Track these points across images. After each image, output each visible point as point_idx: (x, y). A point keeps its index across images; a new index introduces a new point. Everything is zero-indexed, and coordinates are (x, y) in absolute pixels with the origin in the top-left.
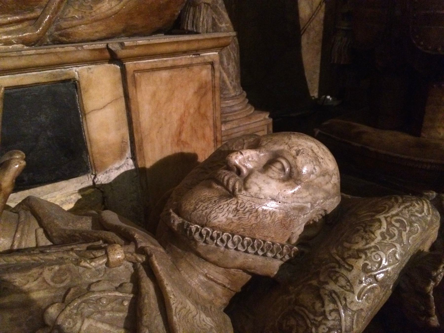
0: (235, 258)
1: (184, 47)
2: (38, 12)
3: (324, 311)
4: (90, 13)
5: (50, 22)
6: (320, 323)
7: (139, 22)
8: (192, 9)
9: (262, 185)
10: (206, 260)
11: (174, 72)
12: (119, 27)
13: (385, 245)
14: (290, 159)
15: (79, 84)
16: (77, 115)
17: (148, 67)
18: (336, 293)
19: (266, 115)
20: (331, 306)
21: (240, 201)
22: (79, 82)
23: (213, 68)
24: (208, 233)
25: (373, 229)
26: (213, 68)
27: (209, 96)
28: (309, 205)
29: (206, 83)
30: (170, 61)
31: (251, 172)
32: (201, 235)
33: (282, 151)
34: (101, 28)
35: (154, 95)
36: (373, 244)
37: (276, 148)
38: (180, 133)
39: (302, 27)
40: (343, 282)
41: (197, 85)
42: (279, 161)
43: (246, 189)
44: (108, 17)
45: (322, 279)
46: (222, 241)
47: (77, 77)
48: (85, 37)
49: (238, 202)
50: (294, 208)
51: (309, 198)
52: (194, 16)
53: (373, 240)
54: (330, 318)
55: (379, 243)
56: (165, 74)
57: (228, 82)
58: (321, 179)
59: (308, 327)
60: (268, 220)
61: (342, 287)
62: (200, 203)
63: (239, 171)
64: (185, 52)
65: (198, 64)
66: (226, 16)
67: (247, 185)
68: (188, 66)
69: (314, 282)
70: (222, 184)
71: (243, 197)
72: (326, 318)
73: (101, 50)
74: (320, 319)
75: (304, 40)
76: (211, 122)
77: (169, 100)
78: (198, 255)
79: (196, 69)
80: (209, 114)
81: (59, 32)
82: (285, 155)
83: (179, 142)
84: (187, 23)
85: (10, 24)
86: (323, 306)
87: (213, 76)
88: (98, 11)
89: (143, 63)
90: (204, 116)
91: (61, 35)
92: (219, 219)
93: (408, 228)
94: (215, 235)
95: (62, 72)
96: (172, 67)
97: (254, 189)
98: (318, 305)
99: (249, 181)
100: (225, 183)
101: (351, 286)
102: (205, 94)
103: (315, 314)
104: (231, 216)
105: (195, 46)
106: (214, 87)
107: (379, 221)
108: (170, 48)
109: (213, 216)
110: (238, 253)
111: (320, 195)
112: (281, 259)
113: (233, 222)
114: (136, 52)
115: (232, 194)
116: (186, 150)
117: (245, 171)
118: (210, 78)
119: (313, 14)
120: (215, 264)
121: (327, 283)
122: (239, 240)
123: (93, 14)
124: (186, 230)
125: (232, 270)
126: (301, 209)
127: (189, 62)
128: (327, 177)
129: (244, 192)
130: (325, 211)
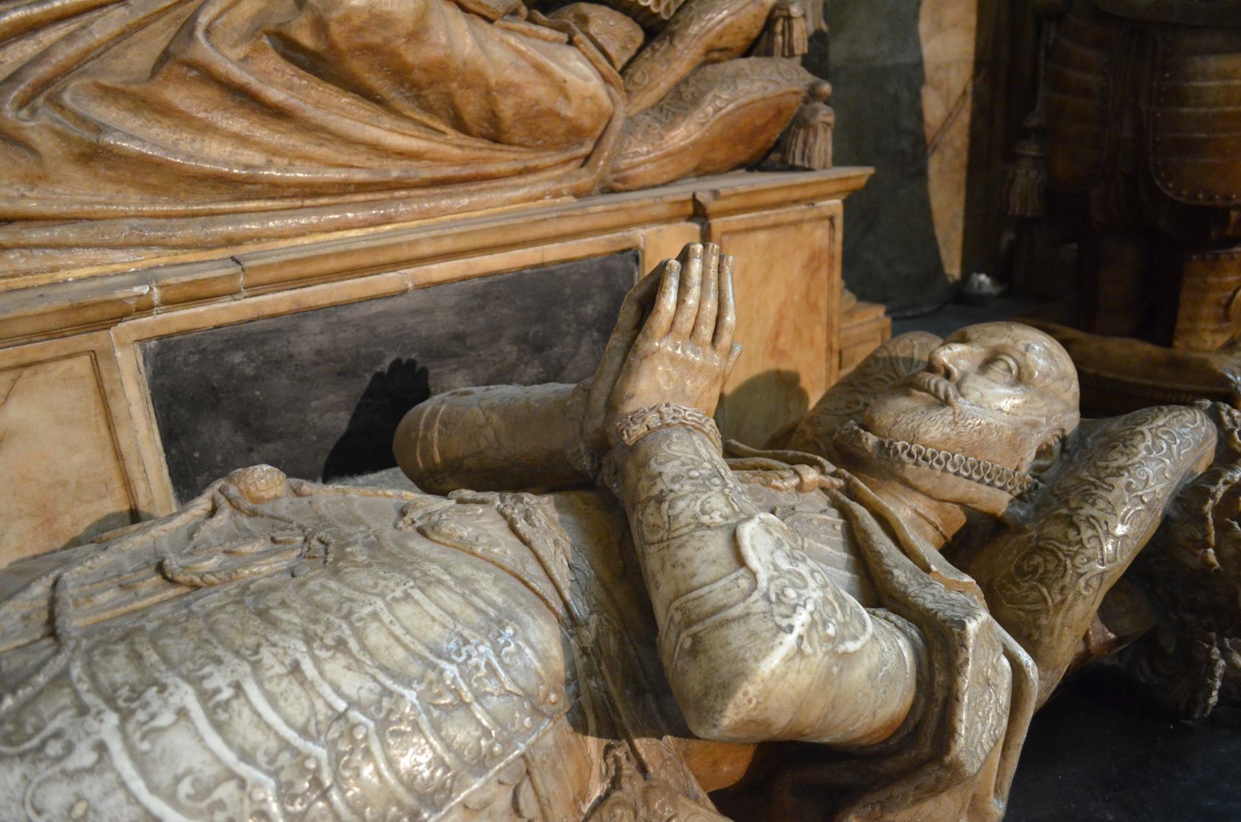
0: (955, 486)
1: (797, 194)
3: (1081, 540)
4: (660, 145)
6: (1077, 553)
8: (802, 132)
9: (985, 391)
10: (915, 489)
11: (776, 234)
12: (691, 163)
13: (1152, 460)
14: (1018, 356)
15: (643, 256)
17: (742, 226)
18: (1093, 517)
19: (879, 311)
20: (1090, 532)
21: (957, 411)
22: (643, 251)
23: (832, 226)
24: (919, 452)
25: (1135, 442)
26: (832, 226)
27: (824, 273)
28: (1044, 420)
30: (772, 216)
31: (964, 375)
32: (910, 455)
33: (1004, 346)
34: (671, 167)
36: (1136, 459)
37: (995, 342)
38: (777, 336)
39: (929, 139)
40: (1101, 504)
42: (1001, 360)
43: (963, 396)
44: (682, 150)
45: (1073, 505)
46: (939, 462)
47: (642, 246)
48: (649, 181)
49: (954, 413)
50: (1026, 424)
51: (1045, 410)
52: (805, 143)
53: (1136, 455)
54: (1088, 546)
55: (1145, 458)
56: (762, 237)
58: (1058, 384)
59: (1060, 560)
60: (994, 437)
61: (1102, 510)
62: (902, 415)
63: (948, 374)
64: (796, 202)
65: (811, 220)
67: (964, 391)
68: (797, 224)
69: (1064, 511)
70: (927, 390)
71: (962, 404)
72: (1083, 546)
73: (683, 203)
74: (1076, 548)
75: (934, 165)
76: (824, 318)
78: (905, 483)
80: (822, 304)
81: (615, 176)
82: (1010, 351)
83: (776, 352)
84: (794, 153)
86: (1079, 533)
87: (832, 239)
88: (671, 142)
89: (736, 220)
90: (814, 308)
91: (616, 180)
92: (932, 435)
93: (1178, 441)
94: (929, 455)
95: (624, 237)
96: (775, 226)
97: (974, 396)
98: (1072, 534)
99: (965, 385)
100: (933, 388)
101: (1113, 508)
102: (818, 268)
103: (1069, 544)
104: (947, 430)
105: (812, 191)
106: (832, 257)
107: (1142, 433)
108: (777, 197)
109: (922, 430)
110: (959, 479)
111: (1058, 407)
112: (1010, 492)
113: (949, 439)
115: (945, 402)
116: (785, 366)
117: (956, 373)
118: (826, 241)
119: (950, 114)
120: (928, 494)
121: (1081, 508)
122: (961, 461)
123: (665, 146)
124: (889, 449)
125: (948, 505)
126: (1034, 425)
127: (799, 217)
128: (1066, 381)
129: (961, 399)
130: (1063, 430)
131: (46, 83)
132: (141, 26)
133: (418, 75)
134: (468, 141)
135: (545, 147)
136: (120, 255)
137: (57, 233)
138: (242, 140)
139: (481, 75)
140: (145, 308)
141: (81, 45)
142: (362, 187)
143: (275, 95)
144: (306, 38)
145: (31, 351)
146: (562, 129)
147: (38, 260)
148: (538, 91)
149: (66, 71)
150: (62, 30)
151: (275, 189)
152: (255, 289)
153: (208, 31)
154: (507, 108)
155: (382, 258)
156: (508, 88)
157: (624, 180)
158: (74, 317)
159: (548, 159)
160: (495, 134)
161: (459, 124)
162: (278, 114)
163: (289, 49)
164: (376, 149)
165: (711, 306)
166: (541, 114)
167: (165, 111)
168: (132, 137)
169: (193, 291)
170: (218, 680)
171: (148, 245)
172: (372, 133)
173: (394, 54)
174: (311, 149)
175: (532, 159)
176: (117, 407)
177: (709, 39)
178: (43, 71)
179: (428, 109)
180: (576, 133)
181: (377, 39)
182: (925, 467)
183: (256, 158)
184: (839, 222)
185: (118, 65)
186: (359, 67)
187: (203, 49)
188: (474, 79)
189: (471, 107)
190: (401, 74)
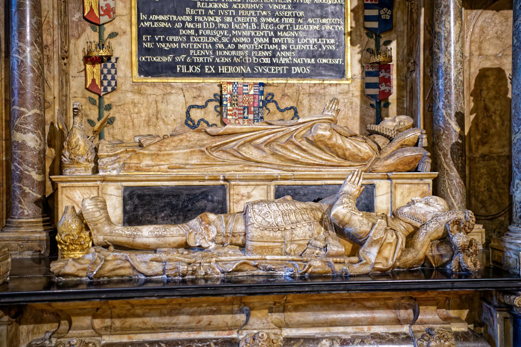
1: (416, 176)
2: (367, 162)
5: (370, 166)
7: (401, 167)
10: (400, 219)
12: (393, 169)
16: (373, 196)
29: (426, 192)
30: (410, 181)
35: (402, 193)
41: (421, 192)
44: (389, 165)
56: (408, 186)
57: (455, 204)
60: (419, 212)
64: (416, 178)
66: (455, 170)
68: (418, 184)
73: (384, 175)
77: (408, 196)
78: (399, 218)
79: (421, 185)
85: (358, 166)
89: (399, 181)
105: (420, 176)
114: (397, 176)
118: (427, 190)
131: (269, 143)
132: (285, 135)
133: (329, 146)
134: (340, 159)
135: (357, 162)
136: (275, 170)
137: (266, 165)
138: (298, 154)
139: (342, 147)
140: (277, 179)
141: (275, 137)
142: (317, 165)
143: (304, 147)
144: (310, 139)
145: (259, 183)
146: (360, 158)
147: (263, 169)
148: (355, 151)
149: (272, 141)
150: (273, 135)
151: (302, 163)
152: (295, 179)
153: (295, 136)
154: (347, 153)
155: (318, 177)
156: (347, 149)
157: (374, 170)
158: (267, 178)
159: (356, 164)
160: (345, 158)
161: (338, 156)
162: (304, 151)
163: (308, 140)
164: (321, 158)
165: (357, 179)
166: (354, 155)
167: (286, 149)
168: (280, 152)
169: (285, 177)
170: (279, 204)
171: (279, 169)
172: (320, 156)
173: (325, 142)
174: (309, 157)
175: (352, 164)
176: (269, 195)
177: (401, 142)
178: (269, 141)
179: (332, 152)
180: (363, 160)
181: (322, 139)
182: (402, 215)
183: (300, 158)
184: (431, 185)
185: (280, 141)
186: (319, 144)
187: (293, 139)
188: (340, 147)
189: (340, 152)
190: (326, 145)
